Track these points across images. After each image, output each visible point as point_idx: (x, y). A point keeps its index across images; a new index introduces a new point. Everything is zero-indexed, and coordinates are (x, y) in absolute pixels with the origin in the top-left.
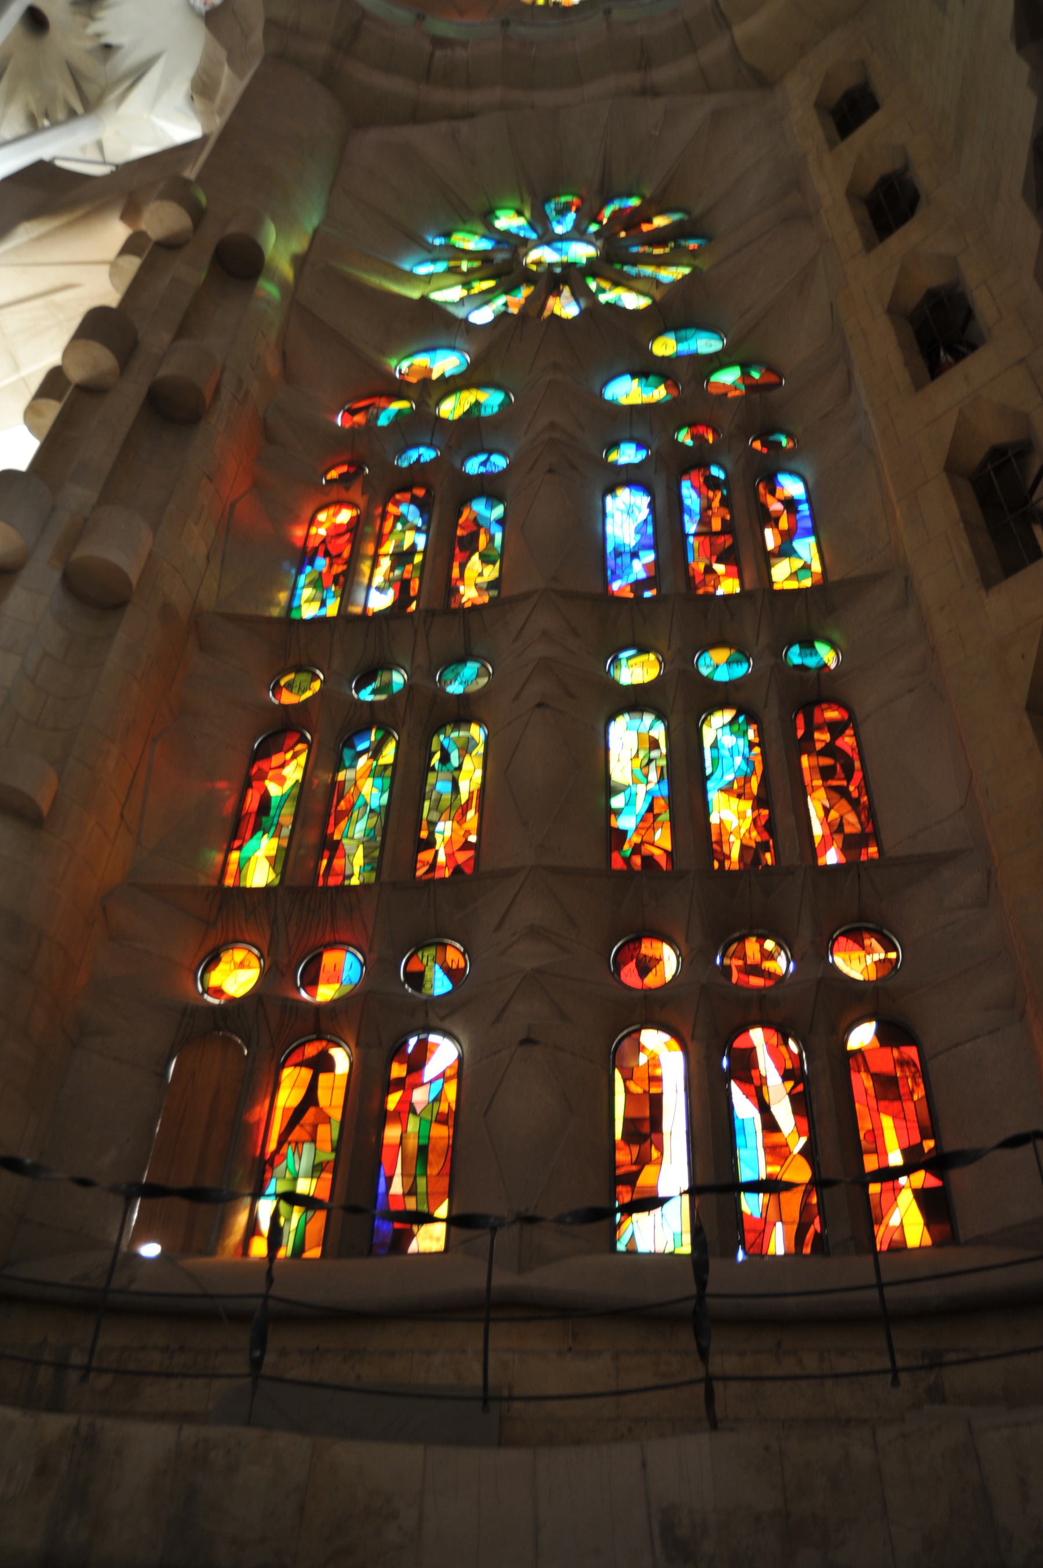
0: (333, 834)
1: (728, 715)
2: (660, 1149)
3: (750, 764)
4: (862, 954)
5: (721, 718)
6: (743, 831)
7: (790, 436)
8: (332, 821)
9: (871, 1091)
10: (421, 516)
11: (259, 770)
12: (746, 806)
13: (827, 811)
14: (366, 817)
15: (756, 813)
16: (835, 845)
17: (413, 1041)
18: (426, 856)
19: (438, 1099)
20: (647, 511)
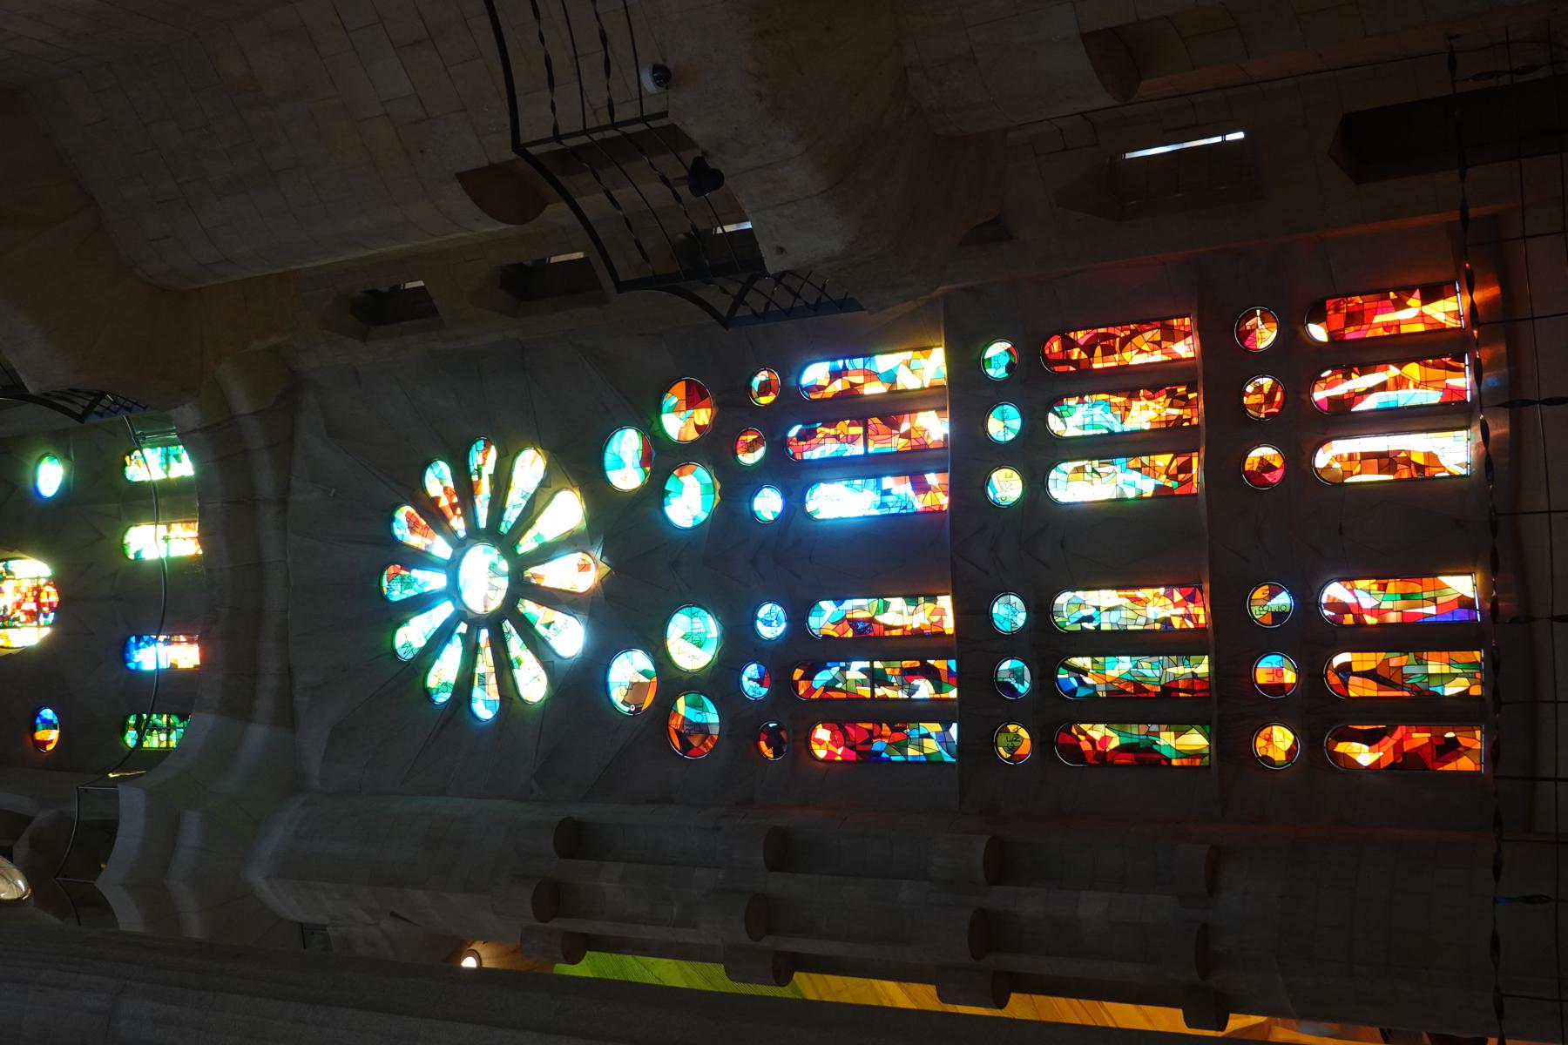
0: (1156, 692)
1: (1051, 417)
2: (1399, 452)
4: (1257, 331)
5: (1054, 423)
6: (1158, 407)
8: (1145, 695)
9: (1357, 328)
10: (830, 668)
11: (1095, 758)
12: (1136, 405)
13: (1141, 351)
15: (1142, 398)
16: (1172, 346)
17: (1327, 613)
18: (1176, 623)
19: (1369, 592)
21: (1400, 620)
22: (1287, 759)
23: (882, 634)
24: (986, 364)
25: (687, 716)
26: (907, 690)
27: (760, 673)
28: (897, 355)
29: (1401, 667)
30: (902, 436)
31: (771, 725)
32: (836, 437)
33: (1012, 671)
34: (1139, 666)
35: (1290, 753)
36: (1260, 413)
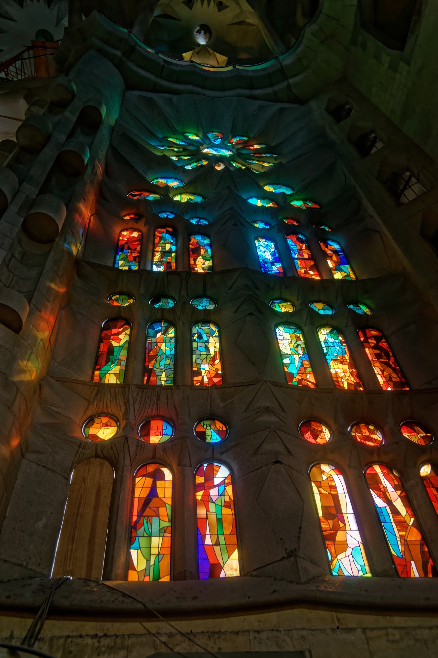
0: (148, 366)
2: (344, 522)
4: (415, 434)
6: (347, 377)
7: (329, 227)
10: (172, 239)
12: (346, 367)
13: (383, 371)
14: (164, 359)
15: (351, 370)
21: (199, 516)
22: (89, 435)
26: (158, 263)
29: (158, 516)
35: (95, 437)
36: (355, 433)
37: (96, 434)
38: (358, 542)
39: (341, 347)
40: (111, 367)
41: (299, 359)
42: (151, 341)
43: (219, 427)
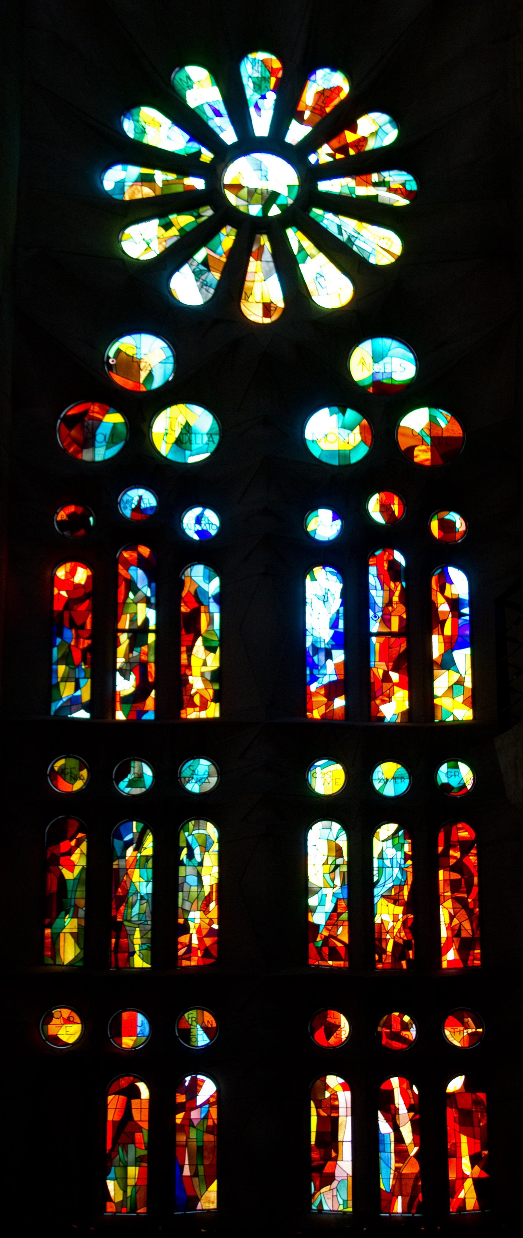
0: (116, 917)
1: (393, 827)
2: (337, 1151)
3: (405, 873)
4: (462, 1028)
5: (387, 829)
6: (396, 931)
8: (114, 906)
9: (457, 1119)
10: (149, 586)
12: (399, 910)
13: (452, 917)
14: (138, 901)
17: (188, 1079)
18: (184, 939)
19: (207, 1117)
20: (340, 601)
23: (182, 643)
24: (452, 763)
25: (102, 424)
27: (146, 509)
28: (469, 672)
30: (386, 675)
31: (91, 519)
32: (390, 603)
33: (141, 776)
34: (143, 901)
35: (56, 1039)
36: (382, 1027)
37: (56, 1035)
38: (347, 1174)
39: (403, 869)
40: (66, 919)
41: (333, 896)
42: (118, 865)
43: (208, 1022)
